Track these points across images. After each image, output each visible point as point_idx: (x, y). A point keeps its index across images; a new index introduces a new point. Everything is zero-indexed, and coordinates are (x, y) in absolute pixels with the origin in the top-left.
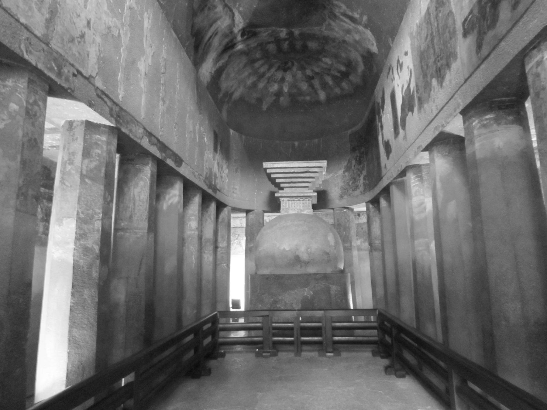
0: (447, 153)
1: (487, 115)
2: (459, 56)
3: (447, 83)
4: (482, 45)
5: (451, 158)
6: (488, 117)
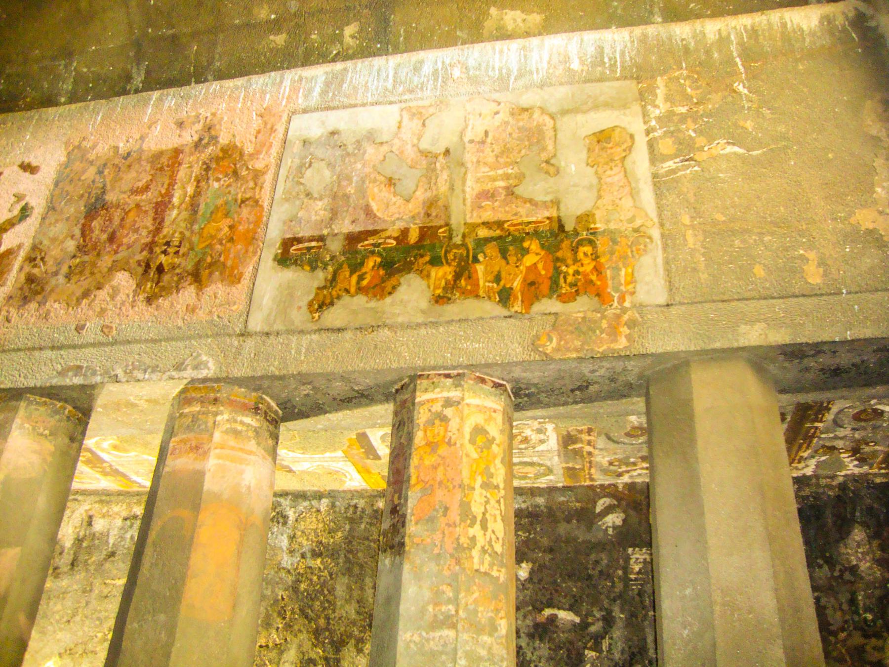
0: (47, 432)
1: (247, 416)
2: (246, 281)
3: (180, 307)
4: (332, 304)
5: (52, 448)
6: (248, 420)
